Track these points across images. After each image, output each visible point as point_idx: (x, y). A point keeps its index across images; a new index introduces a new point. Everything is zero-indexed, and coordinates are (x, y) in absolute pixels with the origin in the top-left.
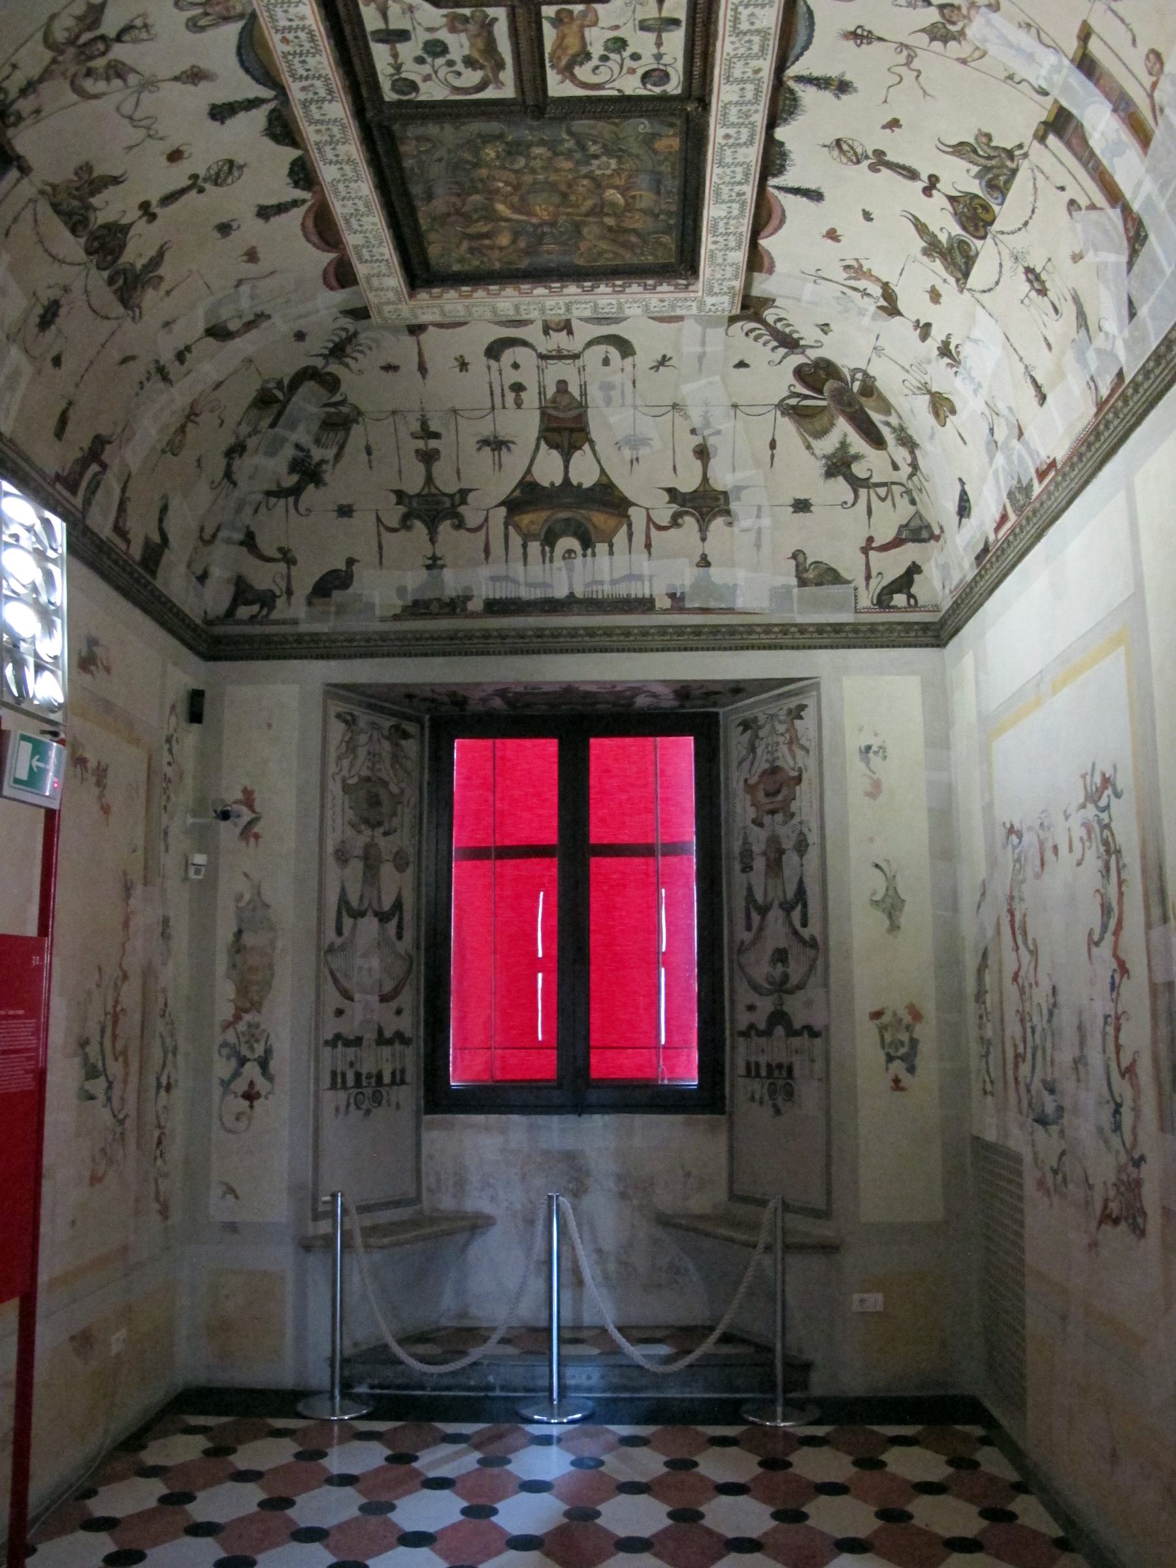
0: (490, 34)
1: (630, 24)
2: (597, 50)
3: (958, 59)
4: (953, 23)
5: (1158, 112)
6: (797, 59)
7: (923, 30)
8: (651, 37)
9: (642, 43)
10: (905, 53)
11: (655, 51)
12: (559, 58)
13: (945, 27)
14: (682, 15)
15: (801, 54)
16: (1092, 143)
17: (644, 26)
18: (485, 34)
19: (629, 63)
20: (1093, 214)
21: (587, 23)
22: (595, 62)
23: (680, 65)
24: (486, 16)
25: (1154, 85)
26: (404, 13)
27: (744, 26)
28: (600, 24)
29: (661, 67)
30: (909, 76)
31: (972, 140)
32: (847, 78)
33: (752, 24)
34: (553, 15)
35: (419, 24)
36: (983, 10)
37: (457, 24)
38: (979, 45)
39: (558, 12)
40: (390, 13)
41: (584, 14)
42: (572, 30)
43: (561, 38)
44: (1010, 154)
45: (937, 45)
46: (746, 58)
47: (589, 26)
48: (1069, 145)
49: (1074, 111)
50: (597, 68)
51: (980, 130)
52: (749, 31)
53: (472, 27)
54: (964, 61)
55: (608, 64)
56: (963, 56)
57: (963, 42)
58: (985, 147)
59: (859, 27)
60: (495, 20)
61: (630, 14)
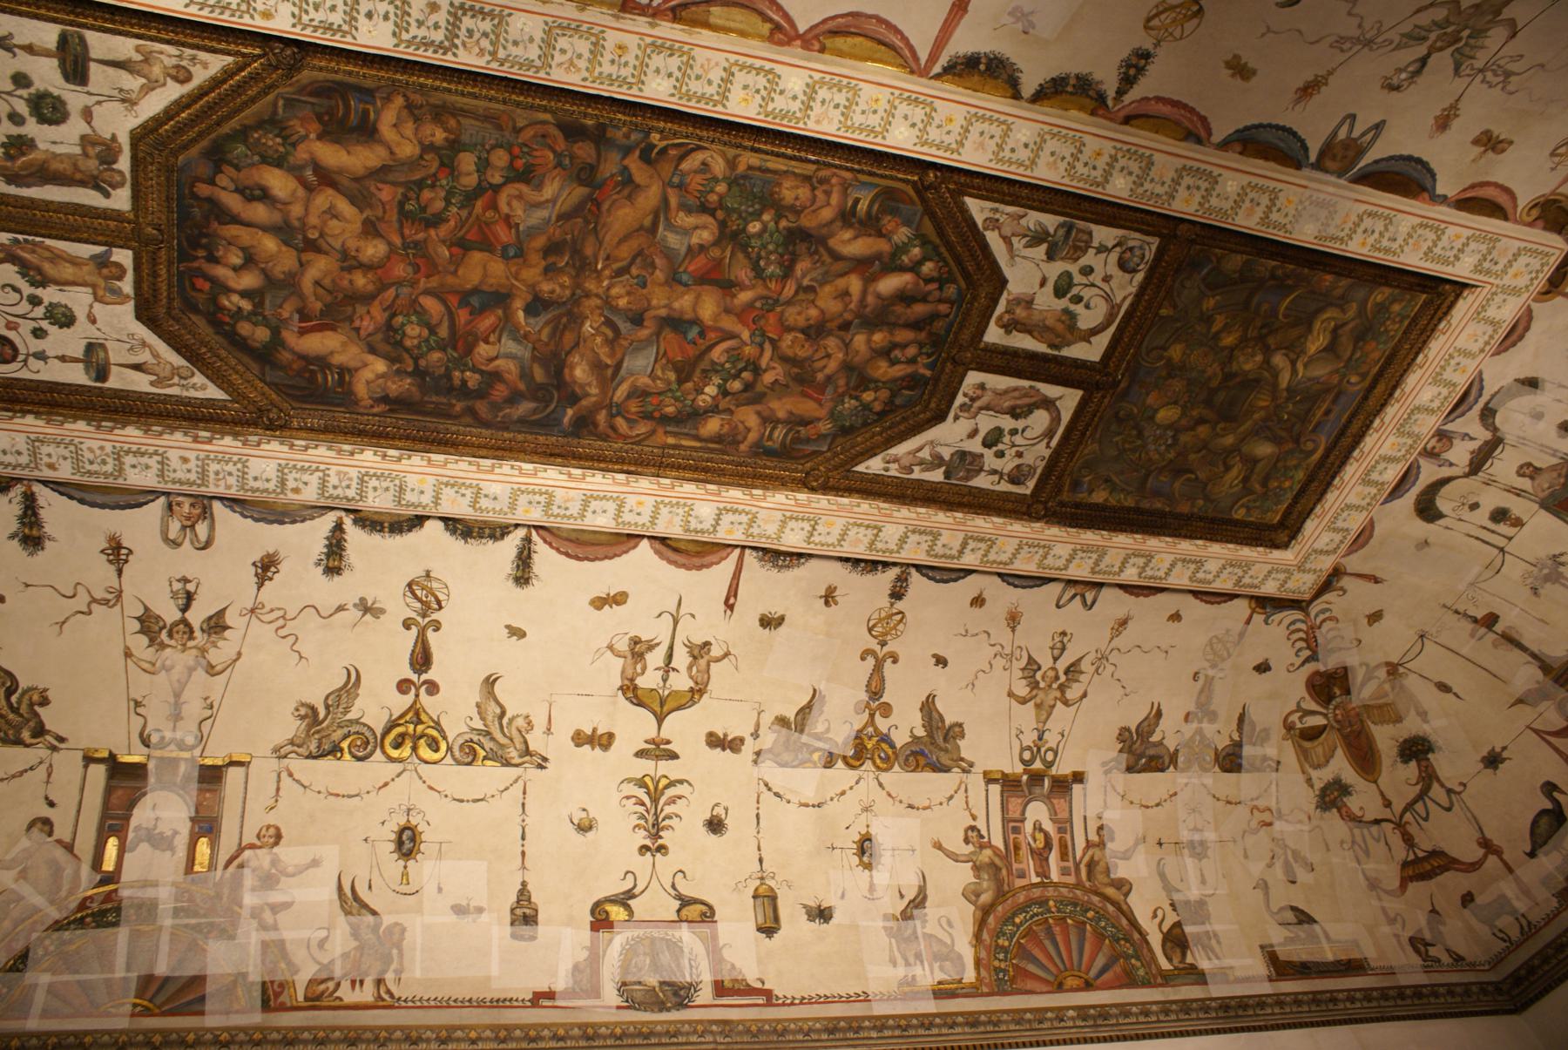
0: (82, 183)
1: (98, 334)
2: (50, 295)
3: (127, 648)
4: (170, 635)
5: (236, 863)
6: (62, 494)
7: (147, 609)
8: (79, 352)
9: (70, 341)
10: (110, 596)
11: (50, 353)
12: (34, 252)
13: (161, 629)
14: (112, 383)
15: (71, 498)
16: (136, 811)
17: (91, 348)
18: (78, 176)
19: (26, 327)
20: (60, 853)
21: (101, 293)
22: (27, 290)
23: (25, 374)
24: (114, 187)
25: (252, 846)
26: (121, 90)
27: (129, 460)
28: (96, 305)
29: (21, 358)
30: (81, 601)
31: (24, 684)
32: (48, 544)
33: (134, 466)
34: (114, 258)
35: (99, 103)
36: (204, 662)
37: (98, 149)
38: (158, 664)
39: (118, 265)
40: (123, 74)
41: (117, 292)
42: (87, 272)
43: (74, 261)
44: (40, 731)
45: (137, 626)
46: (77, 458)
47: (95, 294)
48: (109, 791)
49: (152, 780)
50: (16, 290)
51: (45, 690)
52: (122, 464)
53: (92, 165)
54: (128, 654)
55: (24, 302)
56: (134, 652)
57: (152, 650)
58: (25, 701)
59: (131, 552)
60: (107, 195)
61: (115, 336)
